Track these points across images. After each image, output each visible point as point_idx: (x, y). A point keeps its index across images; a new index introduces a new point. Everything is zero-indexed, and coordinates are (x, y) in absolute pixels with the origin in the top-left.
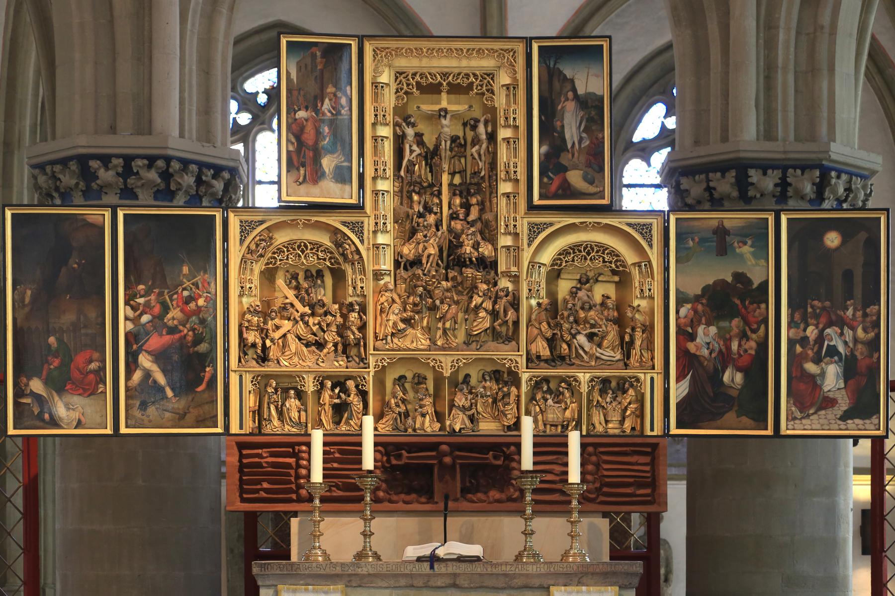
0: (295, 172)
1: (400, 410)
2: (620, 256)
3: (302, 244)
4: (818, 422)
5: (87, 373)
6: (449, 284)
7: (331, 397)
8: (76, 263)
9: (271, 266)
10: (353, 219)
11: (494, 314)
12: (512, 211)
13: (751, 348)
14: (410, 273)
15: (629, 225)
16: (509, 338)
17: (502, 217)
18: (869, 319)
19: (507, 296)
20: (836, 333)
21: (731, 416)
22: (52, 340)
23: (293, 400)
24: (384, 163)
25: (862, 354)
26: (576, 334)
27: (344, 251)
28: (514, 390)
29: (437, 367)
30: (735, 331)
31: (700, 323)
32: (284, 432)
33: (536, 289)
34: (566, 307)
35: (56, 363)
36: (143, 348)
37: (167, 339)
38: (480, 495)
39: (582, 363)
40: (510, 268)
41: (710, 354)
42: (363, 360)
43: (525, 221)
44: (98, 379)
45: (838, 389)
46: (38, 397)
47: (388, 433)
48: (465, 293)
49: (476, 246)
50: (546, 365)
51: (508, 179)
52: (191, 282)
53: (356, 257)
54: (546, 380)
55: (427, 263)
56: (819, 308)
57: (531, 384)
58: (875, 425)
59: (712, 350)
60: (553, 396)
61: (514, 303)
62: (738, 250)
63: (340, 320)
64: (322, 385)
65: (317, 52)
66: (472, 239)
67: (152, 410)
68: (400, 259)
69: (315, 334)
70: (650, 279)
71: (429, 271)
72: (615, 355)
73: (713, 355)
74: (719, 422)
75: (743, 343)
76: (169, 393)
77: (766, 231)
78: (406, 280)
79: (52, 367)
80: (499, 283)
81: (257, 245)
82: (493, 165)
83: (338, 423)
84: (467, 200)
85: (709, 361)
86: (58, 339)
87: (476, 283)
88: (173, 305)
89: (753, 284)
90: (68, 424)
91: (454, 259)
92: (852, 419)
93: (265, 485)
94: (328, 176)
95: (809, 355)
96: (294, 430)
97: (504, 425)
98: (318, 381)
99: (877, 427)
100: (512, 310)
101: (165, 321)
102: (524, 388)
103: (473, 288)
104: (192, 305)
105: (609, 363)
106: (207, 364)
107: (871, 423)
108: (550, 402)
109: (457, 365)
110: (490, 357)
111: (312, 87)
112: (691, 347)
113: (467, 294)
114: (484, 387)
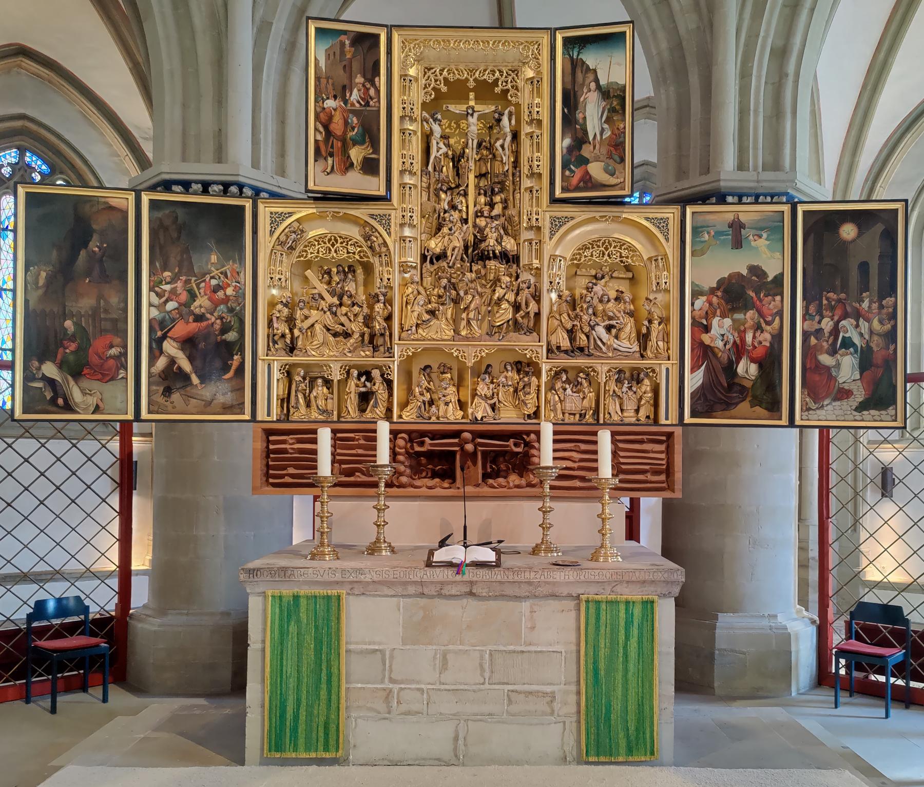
0: (321, 162)
1: (425, 399)
2: (636, 252)
3: (333, 238)
4: (832, 413)
5: (107, 358)
6: (474, 275)
7: (357, 386)
8: (97, 246)
9: (302, 259)
10: (381, 212)
11: (517, 307)
12: (534, 204)
13: (766, 340)
14: (436, 267)
15: (647, 219)
16: (530, 329)
17: (525, 211)
18: (885, 311)
19: (528, 288)
20: (852, 325)
21: (744, 406)
22: (68, 324)
23: (320, 388)
24: (411, 157)
25: (878, 345)
26: (594, 325)
27: (371, 244)
28: (534, 379)
29: (460, 357)
30: (750, 323)
31: (714, 315)
32: (311, 420)
33: (556, 282)
34: (585, 301)
35: (73, 346)
36: (168, 335)
37: (193, 327)
38: (501, 480)
39: (601, 354)
40: (532, 261)
41: (725, 345)
42: (390, 350)
43: (548, 215)
44: (119, 365)
45: (854, 380)
46: (51, 382)
47: (413, 421)
48: (488, 287)
49: (499, 241)
50: (565, 355)
51: (532, 175)
52: (220, 271)
53: (384, 249)
54: (565, 370)
55: (452, 257)
56: (833, 300)
57: (551, 374)
58: (892, 416)
59: (726, 342)
60: (571, 386)
61: (536, 295)
62: (753, 243)
63: (366, 310)
64: (348, 373)
65: (346, 41)
66: (495, 232)
67: (176, 397)
68: (426, 253)
69: (343, 325)
70: (665, 273)
71: (454, 264)
72: (631, 347)
73: (728, 347)
74: (733, 412)
75: (757, 334)
76: (195, 380)
78: (432, 273)
79: (68, 351)
80: (521, 276)
81: (287, 237)
82: (516, 164)
83: (362, 410)
84: (492, 200)
85: (723, 352)
86: (75, 324)
87: (499, 275)
88: (200, 293)
89: (768, 277)
90: (84, 409)
91: (478, 254)
92: (868, 410)
93: (291, 471)
94: (357, 167)
95: (824, 346)
96: (320, 417)
97: (524, 414)
98: (345, 369)
99: (893, 418)
100: (534, 302)
101: (192, 308)
102: (544, 378)
103: (497, 281)
104: (220, 294)
105: (626, 354)
106: (235, 353)
107: (888, 414)
108: (569, 391)
109: (479, 355)
110: (512, 347)
111: (341, 76)
112: (706, 338)
113: (491, 287)
114: (506, 377)
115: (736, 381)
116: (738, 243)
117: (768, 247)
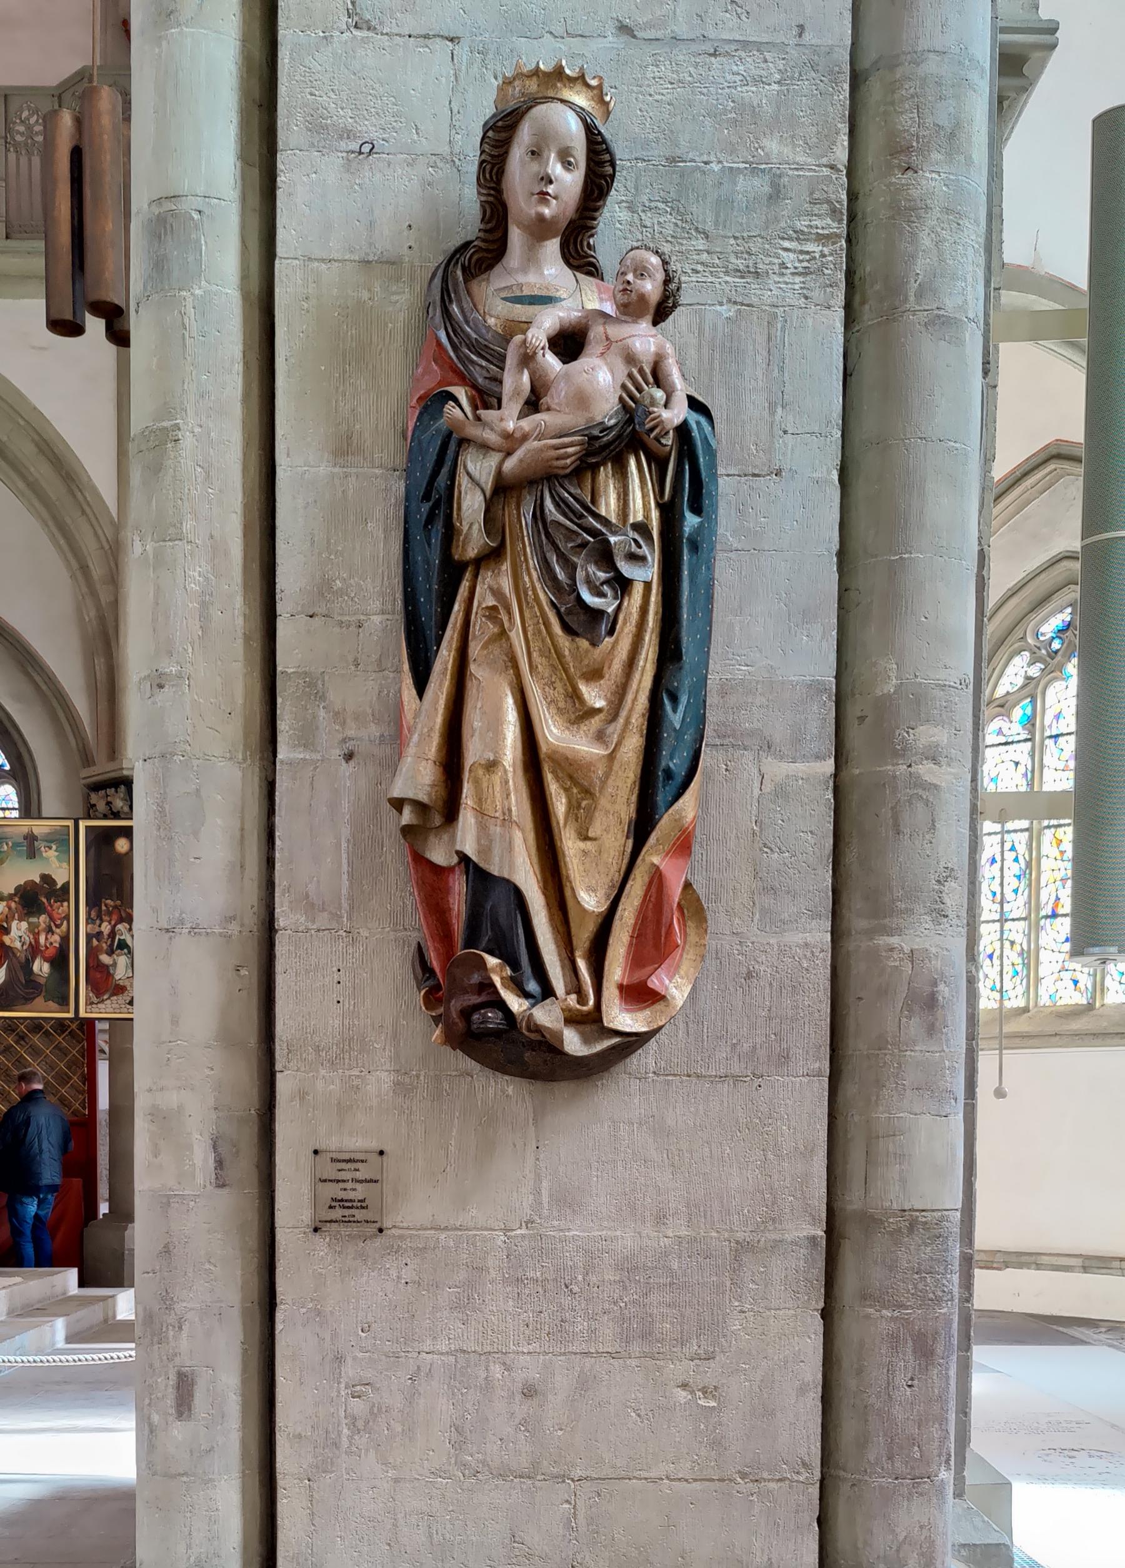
13: (56, 942)
21: (39, 1001)
30: (43, 926)
41: (22, 946)
62: (44, 854)
73: (25, 947)
75: (49, 937)
77: (67, 837)
115: (32, 978)
116: (32, 853)
117: (57, 857)
